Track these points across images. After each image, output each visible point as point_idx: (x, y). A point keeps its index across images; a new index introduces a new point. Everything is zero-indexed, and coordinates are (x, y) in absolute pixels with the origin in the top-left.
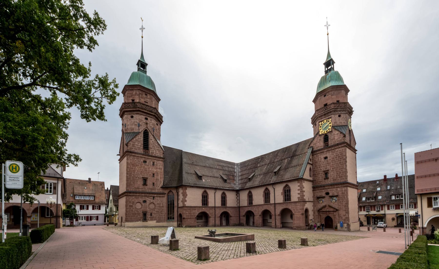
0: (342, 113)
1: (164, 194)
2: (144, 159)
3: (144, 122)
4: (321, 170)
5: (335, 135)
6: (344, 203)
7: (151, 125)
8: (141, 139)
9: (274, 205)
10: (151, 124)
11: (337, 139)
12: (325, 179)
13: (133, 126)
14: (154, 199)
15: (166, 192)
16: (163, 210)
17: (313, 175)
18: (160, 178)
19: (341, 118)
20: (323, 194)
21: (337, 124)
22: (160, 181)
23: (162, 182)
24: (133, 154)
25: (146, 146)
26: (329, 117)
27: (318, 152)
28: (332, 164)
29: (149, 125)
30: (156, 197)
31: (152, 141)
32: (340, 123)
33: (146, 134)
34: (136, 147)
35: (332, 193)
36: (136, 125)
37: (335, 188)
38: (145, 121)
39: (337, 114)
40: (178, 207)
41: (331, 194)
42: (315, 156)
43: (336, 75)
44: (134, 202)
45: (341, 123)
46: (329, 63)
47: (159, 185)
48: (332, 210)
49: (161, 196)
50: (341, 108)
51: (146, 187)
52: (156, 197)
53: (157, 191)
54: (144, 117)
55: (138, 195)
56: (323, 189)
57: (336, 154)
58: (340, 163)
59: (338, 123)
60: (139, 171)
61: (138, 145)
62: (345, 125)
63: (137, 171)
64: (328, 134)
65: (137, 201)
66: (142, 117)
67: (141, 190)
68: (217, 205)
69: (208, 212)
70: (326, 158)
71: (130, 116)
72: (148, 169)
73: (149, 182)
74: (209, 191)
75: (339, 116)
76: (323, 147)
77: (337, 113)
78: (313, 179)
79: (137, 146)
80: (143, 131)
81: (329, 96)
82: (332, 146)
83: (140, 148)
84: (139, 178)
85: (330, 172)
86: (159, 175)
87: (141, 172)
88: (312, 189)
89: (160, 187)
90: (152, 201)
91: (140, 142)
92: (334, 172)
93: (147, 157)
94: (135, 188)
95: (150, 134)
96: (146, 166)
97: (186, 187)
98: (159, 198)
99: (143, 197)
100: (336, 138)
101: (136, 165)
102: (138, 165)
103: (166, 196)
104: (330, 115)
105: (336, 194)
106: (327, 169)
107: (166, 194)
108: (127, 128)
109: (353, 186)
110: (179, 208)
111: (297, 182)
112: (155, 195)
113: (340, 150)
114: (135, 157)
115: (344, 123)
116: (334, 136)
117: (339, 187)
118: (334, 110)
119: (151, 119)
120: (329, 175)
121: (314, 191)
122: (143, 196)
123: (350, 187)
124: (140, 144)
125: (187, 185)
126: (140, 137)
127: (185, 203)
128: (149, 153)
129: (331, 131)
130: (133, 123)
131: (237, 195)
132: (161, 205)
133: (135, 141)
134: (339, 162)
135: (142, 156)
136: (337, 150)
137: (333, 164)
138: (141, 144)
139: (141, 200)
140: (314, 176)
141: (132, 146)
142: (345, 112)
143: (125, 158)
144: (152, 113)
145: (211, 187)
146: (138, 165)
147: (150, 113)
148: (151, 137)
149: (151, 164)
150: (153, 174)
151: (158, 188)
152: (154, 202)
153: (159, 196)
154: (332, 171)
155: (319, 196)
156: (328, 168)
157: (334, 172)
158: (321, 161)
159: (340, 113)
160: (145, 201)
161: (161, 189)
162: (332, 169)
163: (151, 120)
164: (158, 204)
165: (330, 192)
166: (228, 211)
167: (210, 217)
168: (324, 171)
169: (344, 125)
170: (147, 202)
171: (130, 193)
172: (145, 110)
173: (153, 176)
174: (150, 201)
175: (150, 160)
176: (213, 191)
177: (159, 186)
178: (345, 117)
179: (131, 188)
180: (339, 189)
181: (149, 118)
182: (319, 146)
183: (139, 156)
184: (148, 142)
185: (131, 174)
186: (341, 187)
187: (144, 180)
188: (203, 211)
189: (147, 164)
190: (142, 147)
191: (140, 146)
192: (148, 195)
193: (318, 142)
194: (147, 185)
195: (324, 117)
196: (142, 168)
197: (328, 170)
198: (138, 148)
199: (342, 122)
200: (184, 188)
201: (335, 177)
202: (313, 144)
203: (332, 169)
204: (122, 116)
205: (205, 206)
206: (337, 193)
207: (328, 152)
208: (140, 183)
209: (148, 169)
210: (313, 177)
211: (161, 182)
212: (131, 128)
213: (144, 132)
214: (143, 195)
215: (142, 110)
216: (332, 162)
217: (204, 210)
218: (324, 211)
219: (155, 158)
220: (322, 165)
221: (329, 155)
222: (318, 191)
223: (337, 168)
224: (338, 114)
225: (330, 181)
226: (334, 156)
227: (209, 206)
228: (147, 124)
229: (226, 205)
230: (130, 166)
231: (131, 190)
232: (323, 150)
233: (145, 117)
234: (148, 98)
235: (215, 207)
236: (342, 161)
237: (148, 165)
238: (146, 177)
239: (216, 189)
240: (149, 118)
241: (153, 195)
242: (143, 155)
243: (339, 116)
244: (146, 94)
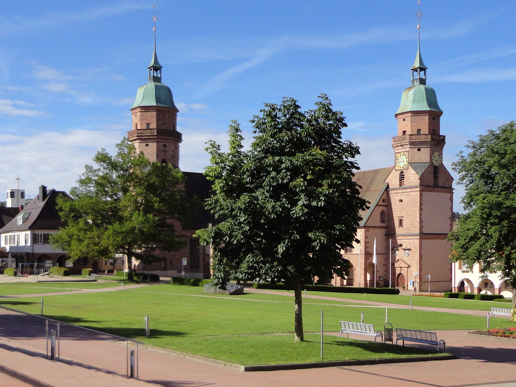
5: (410, 174)
11: (413, 180)
21: (414, 161)
28: (406, 209)
35: (406, 246)
39: (415, 148)
57: (411, 198)
58: (414, 210)
75: (419, 150)
78: (387, 224)
81: (408, 121)
92: (408, 220)
100: (412, 179)
105: (409, 248)
106: (402, 215)
113: (414, 195)
116: (410, 175)
120: (404, 222)
134: (413, 209)
136: (412, 193)
137: (407, 211)
140: (388, 221)
154: (406, 218)
156: (403, 214)
157: (408, 220)
158: (396, 203)
169: (424, 162)
182: (395, 184)
201: (409, 226)
206: (410, 245)
210: (387, 222)
216: (407, 208)
220: (397, 209)
223: (411, 216)
224: (417, 148)
226: (409, 200)
236: (416, 208)
243: (419, 150)
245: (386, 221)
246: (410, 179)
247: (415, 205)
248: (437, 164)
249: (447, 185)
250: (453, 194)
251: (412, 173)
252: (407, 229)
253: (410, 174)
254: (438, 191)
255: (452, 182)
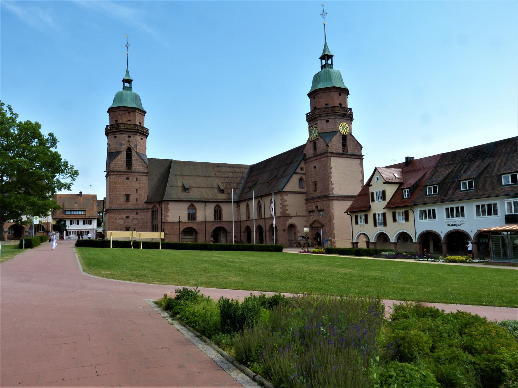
0: (331, 118)
1: (148, 209)
2: (126, 176)
3: (127, 141)
4: (312, 180)
6: (328, 218)
7: (134, 142)
8: (123, 157)
9: (264, 220)
10: (134, 140)
12: (315, 191)
13: (116, 146)
14: (137, 215)
15: (150, 206)
16: (147, 225)
17: (306, 186)
18: (144, 194)
19: (328, 123)
20: (314, 208)
21: (324, 131)
22: (144, 196)
23: (147, 197)
24: (116, 173)
25: (129, 162)
26: (316, 122)
27: (309, 161)
28: (319, 174)
29: (131, 142)
30: (139, 212)
31: (135, 158)
32: (328, 129)
33: (129, 151)
34: (118, 166)
36: (119, 144)
37: (321, 201)
38: (127, 139)
39: (323, 119)
40: (162, 223)
41: (319, 208)
42: (307, 164)
43: (326, 74)
44: (116, 218)
45: (330, 129)
46: (326, 57)
47: (143, 200)
48: (319, 225)
49: (145, 211)
50: (327, 113)
51: (129, 203)
52: (139, 212)
53: (140, 206)
54: (127, 135)
55: (120, 211)
56: (313, 202)
59: (326, 130)
60: (122, 188)
61: (120, 164)
62: (334, 131)
63: (120, 188)
64: (316, 141)
65: (119, 217)
66: (124, 136)
67: (123, 207)
68: (208, 220)
69: (196, 228)
70: (315, 167)
71: (113, 136)
72: (131, 185)
73: (132, 198)
74: (196, 205)
76: (312, 155)
77: (324, 118)
78: (306, 190)
79: (119, 165)
80: (126, 149)
82: (322, 154)
83: (122, 166)
84: (121, 195)
85: (318, 183)
86: (143, 190)
87: (123, 188)
88: (304, 202)
89: (143, 202)
90: (135, 216)
91: (122, 160)
93: (130, 174)
94: (118, 205)
95: (133, 151)
96: (128, 183)
97: (168, 202)
98: (142, 213)
99: (126, 213)
100: (322, 146)
101: (119, 183)
102: (121, 183)
103: (150, 210)
104: (316, 121)
106: (316, 180)
107: (150, 209)
108: (111, 148)
109: (338, 199)
110: (163, 224)
111: (279, 195)
112: (139, 211)
113: (324, 160)
114: (118, 175)
115: (333, 128)
117: (324, 201)
118: (319, 115)
119: (134, 136)
121: (307, 204)
122: (125, 212)
123: (334, 200)
124: (122, 163)
125: (168, 200)
126: (123, 155)
127: (167, 218)
128: (132, 170)
129: (318, 139)
130: (116, 143)
131: (237, 207)
132: (145, 220)
133: (117, 160)
135: (124, 173)
136: (322, 159)
138: (123, 162)
139: (124, 216)
141: (114, 166)
142: (334, 117)
143: (108, 177)
144: (135, 131)
145: (199, 200)
146: (121, 183)
147: (133, 131)
148: (134, 153)
149: (134, 180)
150: (137, 190)
151: (142, 203)
152: (137, 218)
153: (143, 211)
155: (311, 210)
159: (327, 118)
160: (127, 217)
161: (145, 204)
162: (319, 181)
163: (134, 137)
164: (142, 219)
165: (318, 205)
166: (224, 226)
167: (199, 233)
168: (314, 182)
170: (130, 218)
171: (113, 209)
172: (127, 129)
173: (137, 192)
174: (133, 217)
175: (133, 176)
176: (203, 205)
177: (142, 202)
178: (334, 122)
179: (114, 205)
180: (324, 203)
181: (132, 136)
183: (122, 173)
184: (131, 159)
185: (113, 192)
186: (326, 200)
187: (126, 196)
188: (189, 226)
189: (130, 180)
190: (125, 165)
191: (123, 164)
192: (130, 211)
193: (310, 149)
194: (129, 201)
195: (312, 123)
196: (125, 185)
197: (317, 181)
198: (120, 166)
199: (331, 127)
200: (165, 203)
202: (306, 151)
203: (319, 181)
204: (107, 134)
205: (193, 221)
207: (316, 161)
208: (123, 199)
209: (131, 185)
211: (145, 197)
212: (114, 148)
213: (127, 150)
214: (126, 211)
215: (124, 130)
217: (190, 225)
218: (314, 227)
219: (138, 174)
221: (316, 164)
222: (310, 204)
225: (318, 194)
227: (197, 221)
228: (129, 141)
229: (222, 219)
230: (113, 184)
231: (114, 206)
232: (312, 158)
233: (128, 135)
234: (131, 116)
235: (205, 222)
237: (131, 182)
238: (128, 193)
239: (205, 202)
240: (132, 136)
241: (136, 211)
242: (126, 172)
243: (327, 121)
244: (130, 113)
245: (305, 187)
246: (320, 147)
247: (325, 169)
248: (344, 133)
249: (356, 152)
250: (363, 160)
251: (321, 142)
252: (321, 192)
253: (320, 143)
254: (347, 157)
255: (361, 149)
